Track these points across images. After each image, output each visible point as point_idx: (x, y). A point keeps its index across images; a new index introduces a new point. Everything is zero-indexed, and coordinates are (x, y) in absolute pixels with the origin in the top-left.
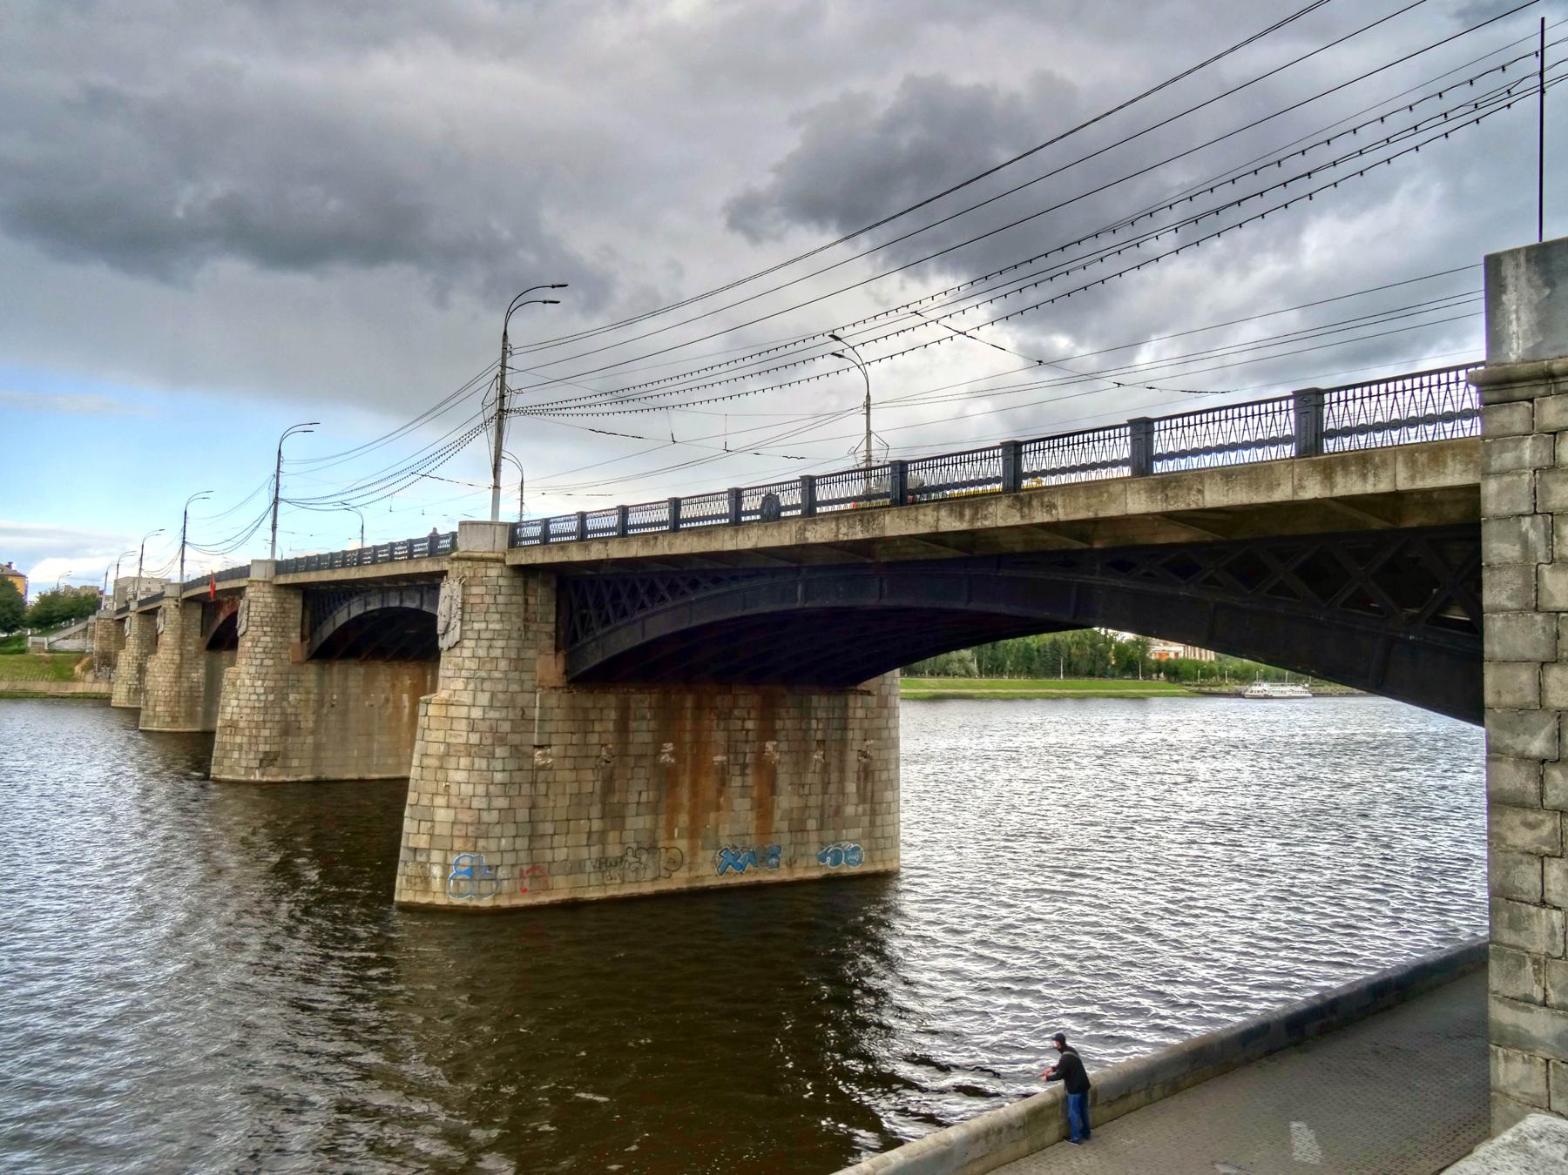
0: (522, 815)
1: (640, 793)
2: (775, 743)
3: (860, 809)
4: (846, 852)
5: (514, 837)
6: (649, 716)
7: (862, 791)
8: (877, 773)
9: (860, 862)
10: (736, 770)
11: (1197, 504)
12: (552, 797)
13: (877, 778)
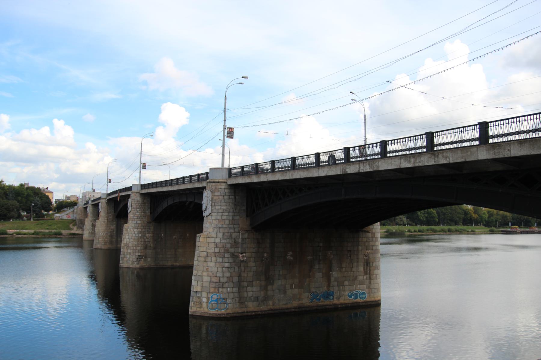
0: (236, 279)
1: (279, 271)
2: (331, 251)
6: (282, 242)
7: (366, 270)
8: (371, 263)
9: (365, 298)
11: (508, 155)
13: (371, 265)
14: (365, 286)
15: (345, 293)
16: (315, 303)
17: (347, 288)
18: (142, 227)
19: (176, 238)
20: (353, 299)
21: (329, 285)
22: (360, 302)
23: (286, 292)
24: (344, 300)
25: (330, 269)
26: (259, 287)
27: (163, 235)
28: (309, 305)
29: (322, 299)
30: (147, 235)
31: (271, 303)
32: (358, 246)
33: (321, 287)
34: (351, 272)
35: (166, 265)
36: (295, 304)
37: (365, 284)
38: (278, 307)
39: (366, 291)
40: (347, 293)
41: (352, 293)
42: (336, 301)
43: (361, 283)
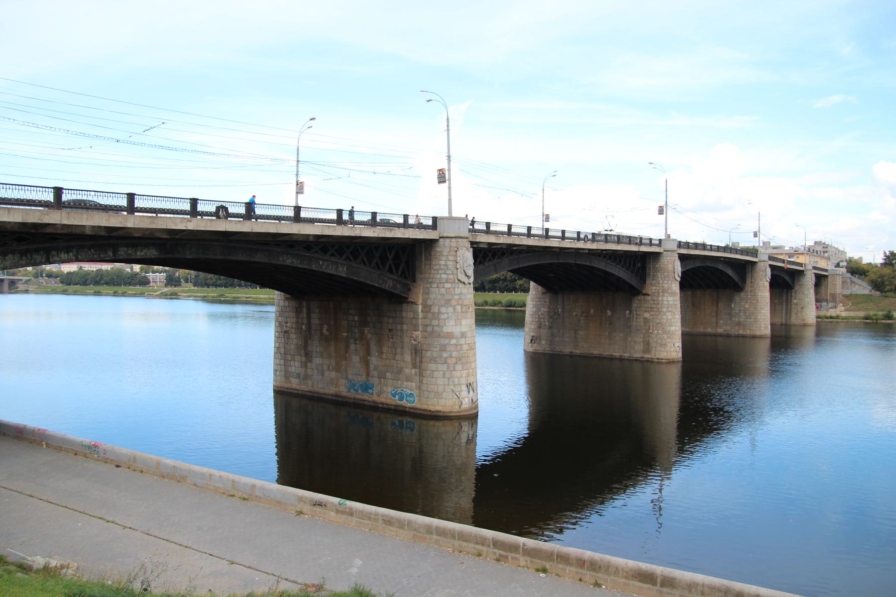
2: (368, 329)
7: (414, 362)
8: (424, 352)
9: (413, 402)
10: (352, 341)
12: (289, 345)
13: (424, 355)
14: (414, 384)
15: (387, 389)
16: (352, 394)
17: (390, 382)
18: (537, 300)
19: (576, 315)
20: (396, 401)
21: (368, 374)
22: (406, 407)
23: (324, 373)
24: (386, 398)
25: (368, 352)
26: (300, 363)
27: (560, 310)
28: (346, 395)
29: (360, 391)
30: (542, 309)
31: (310, 383)
32: (402, 324)
34: (394, 361)
35: (563, 352)
36: (331, 390)
37: (413, 382)
38: (316, 390)
39: (415, 393)
40: (389, 389)
41: (396, 390)
42: (375, 398)
43: (409, 379)
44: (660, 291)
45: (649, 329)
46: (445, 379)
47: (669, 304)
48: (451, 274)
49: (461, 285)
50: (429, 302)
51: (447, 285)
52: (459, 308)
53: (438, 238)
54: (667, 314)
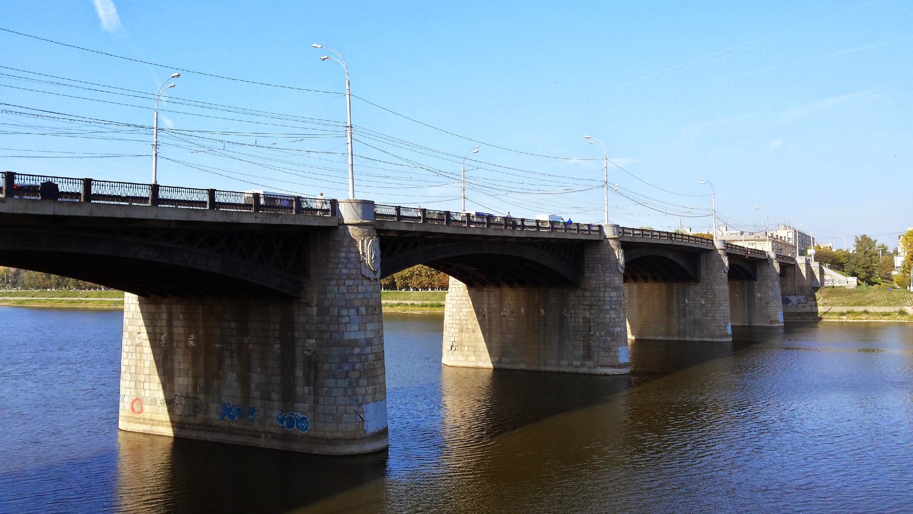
0: (133, 370)
1: (180, 363)
2: (249, 338)
3: (306, 389)
4: (297, 419)
5: (130, 381)
8: (319, 365)
9: (306, 429)
12: (143, 361)
29: (236, 418)
33: (236, 397)
39: (309, 416)
44: (601, 285)
45: (590, 331)
46: (346, 398)
47: (612, 300)
48: (353, 269)
49: (365, 282)
50: (327, 304)
51: (348, 282)
52: (363, 310)
53: (337, 225)
54: (610, 312)
